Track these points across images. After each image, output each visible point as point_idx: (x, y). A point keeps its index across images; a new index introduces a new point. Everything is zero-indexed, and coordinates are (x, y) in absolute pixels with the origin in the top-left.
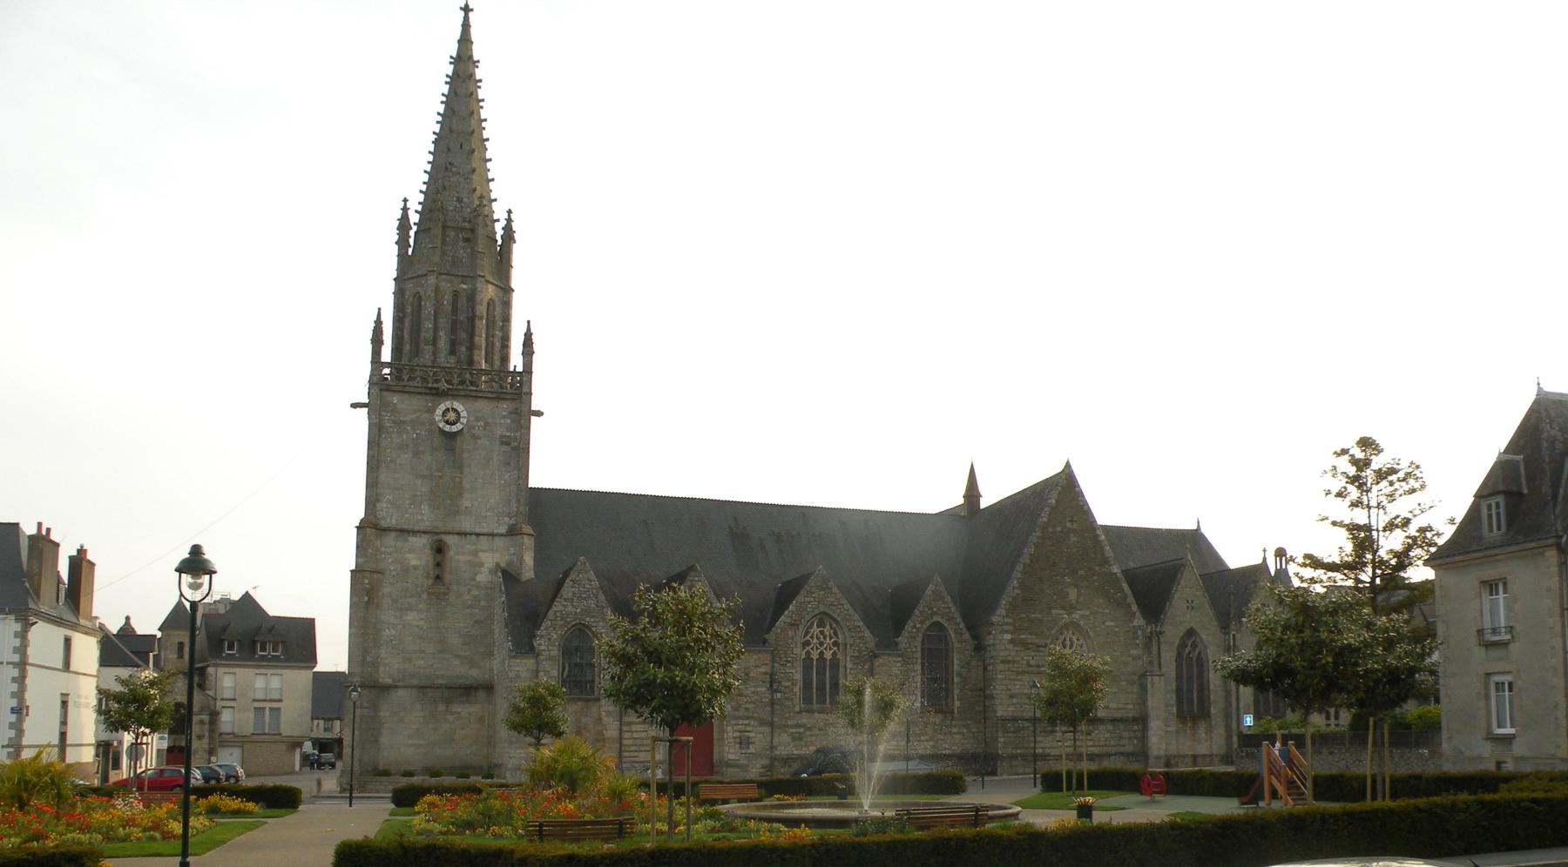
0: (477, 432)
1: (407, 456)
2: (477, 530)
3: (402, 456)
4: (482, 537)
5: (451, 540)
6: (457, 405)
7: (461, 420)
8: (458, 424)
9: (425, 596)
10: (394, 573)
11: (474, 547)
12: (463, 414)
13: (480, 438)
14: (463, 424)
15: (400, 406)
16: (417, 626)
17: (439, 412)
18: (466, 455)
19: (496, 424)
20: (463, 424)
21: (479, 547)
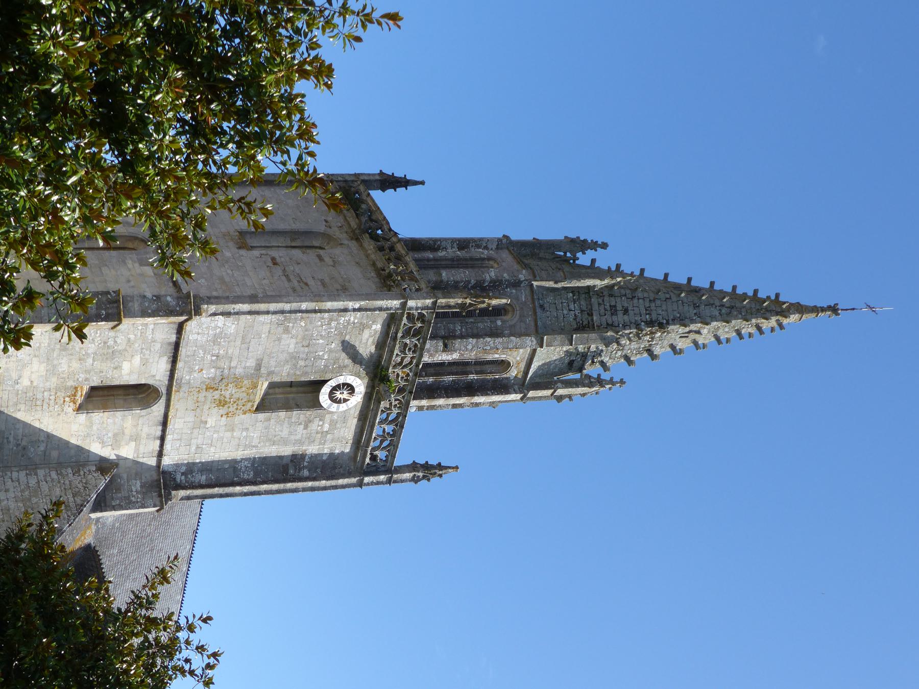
0: (315, 426)
1: (292, 346)
2: (169, 438)
3: (294, 341)
4: (158, 442)
5: (158, 409)
6: (357, 400)
7: (335, 405)
8: (329, 402)
9: (70, 383)
10: (111, 342)
11: (144, 435)
12: (343, 407)
13: (306, 427)
14: (329, 407)
15: (366, 334)
16: (20, 377)
17: (350, 379)
18: (282, 414)
19: (324, 444)
20: (329, 407)
21: (143, 441)
